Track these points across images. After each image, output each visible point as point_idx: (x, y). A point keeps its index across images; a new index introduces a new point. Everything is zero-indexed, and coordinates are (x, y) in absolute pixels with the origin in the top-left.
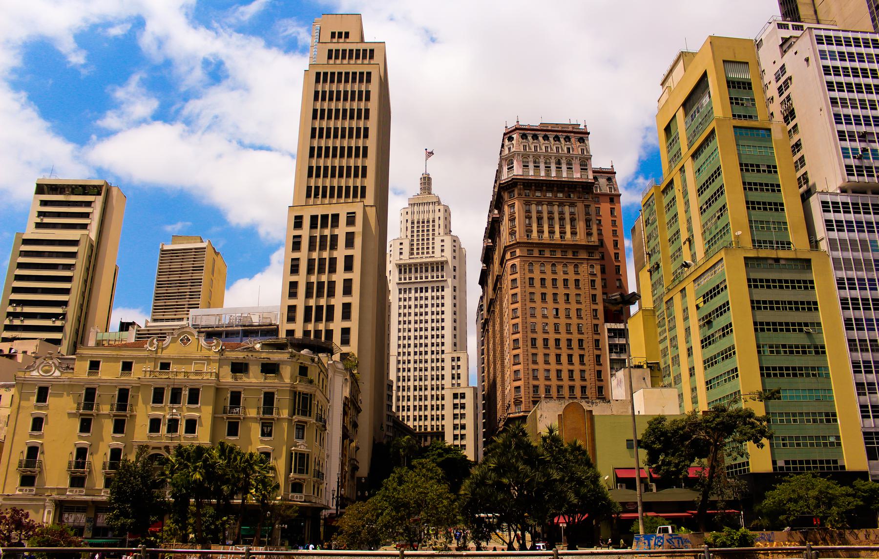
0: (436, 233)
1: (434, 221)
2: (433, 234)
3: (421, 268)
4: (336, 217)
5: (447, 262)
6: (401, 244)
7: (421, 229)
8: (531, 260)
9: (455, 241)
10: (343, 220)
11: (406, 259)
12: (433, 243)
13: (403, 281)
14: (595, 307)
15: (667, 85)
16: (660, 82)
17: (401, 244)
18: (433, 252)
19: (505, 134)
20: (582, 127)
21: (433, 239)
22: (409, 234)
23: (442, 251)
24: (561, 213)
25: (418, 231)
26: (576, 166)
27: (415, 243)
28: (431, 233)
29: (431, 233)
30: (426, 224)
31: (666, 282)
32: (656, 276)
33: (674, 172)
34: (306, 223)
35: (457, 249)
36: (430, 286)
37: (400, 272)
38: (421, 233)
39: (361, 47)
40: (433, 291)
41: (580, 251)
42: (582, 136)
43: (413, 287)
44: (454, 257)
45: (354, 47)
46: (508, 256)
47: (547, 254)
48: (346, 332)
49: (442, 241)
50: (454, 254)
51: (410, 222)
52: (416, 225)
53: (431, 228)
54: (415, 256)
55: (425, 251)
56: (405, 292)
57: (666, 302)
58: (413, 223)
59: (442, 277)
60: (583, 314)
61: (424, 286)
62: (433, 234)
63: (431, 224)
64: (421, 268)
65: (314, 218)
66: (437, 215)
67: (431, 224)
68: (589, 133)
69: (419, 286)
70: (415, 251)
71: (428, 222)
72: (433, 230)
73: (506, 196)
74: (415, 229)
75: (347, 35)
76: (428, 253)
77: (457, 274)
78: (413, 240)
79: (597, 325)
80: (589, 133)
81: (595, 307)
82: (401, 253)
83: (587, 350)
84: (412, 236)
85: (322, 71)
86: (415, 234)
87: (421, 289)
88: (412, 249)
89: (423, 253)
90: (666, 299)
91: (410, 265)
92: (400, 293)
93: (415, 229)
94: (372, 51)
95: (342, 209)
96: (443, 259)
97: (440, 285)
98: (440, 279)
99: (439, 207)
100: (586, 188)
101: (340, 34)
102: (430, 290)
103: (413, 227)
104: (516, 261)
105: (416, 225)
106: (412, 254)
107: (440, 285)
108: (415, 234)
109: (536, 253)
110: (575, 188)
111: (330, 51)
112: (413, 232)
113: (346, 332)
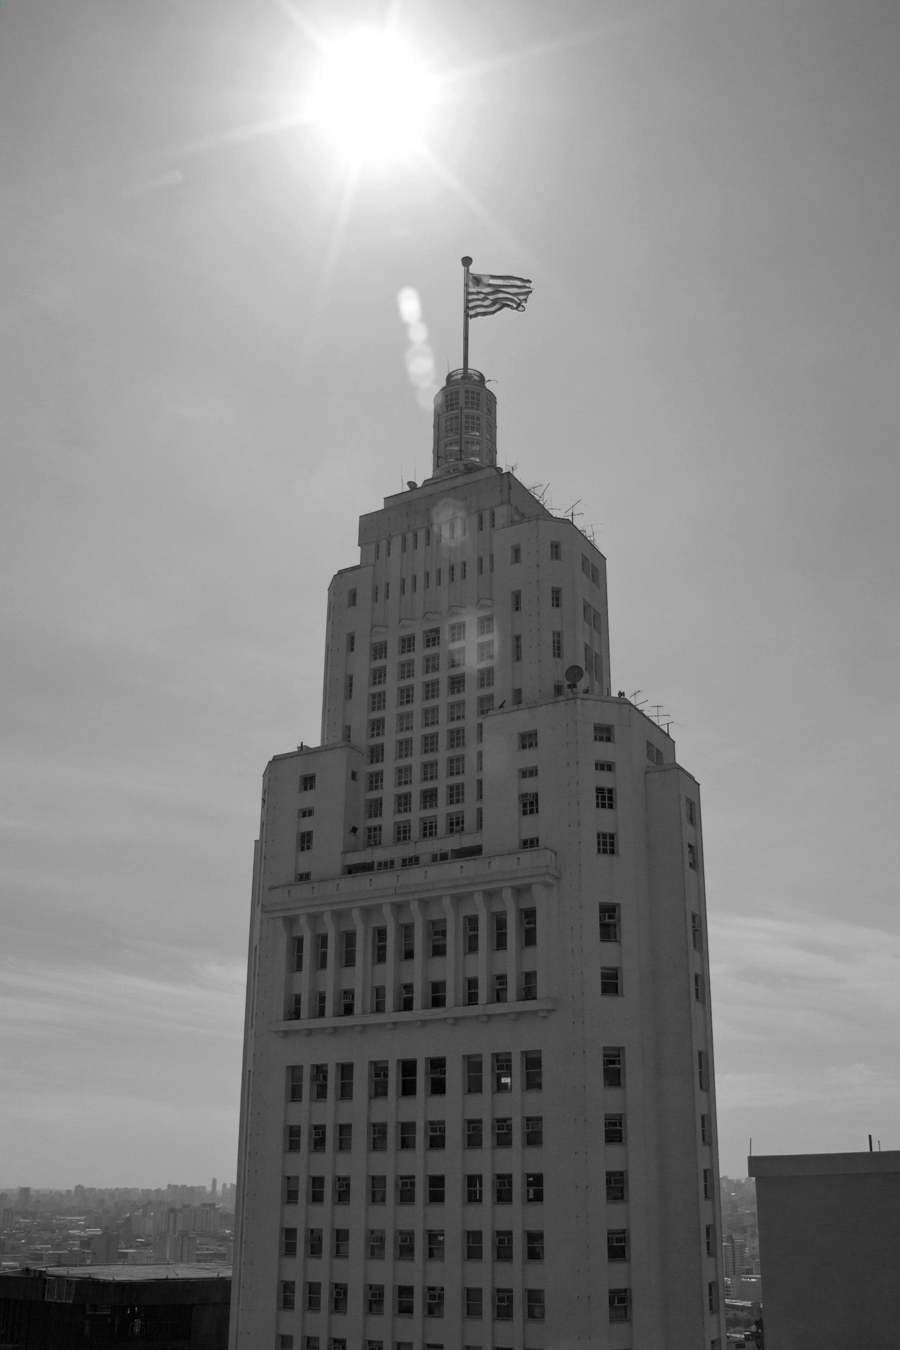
23: (529, 805)
25: (406, 695)
44: (607, 844)
49: (528, 740)
50: (605, 821)
52: (392, 661)
58: (379, 651)
69: (392, 1050)
70: (388, 820)
74: (392, 685)
77: (629, 955)
78: (376, 753)
82: (305, 841)
84: (377, 726)
88: (375, 808)
93: (392, 685)
97: (515, 1041)
103: (378, 676)
108: (391, 712)
112: (377, 702)
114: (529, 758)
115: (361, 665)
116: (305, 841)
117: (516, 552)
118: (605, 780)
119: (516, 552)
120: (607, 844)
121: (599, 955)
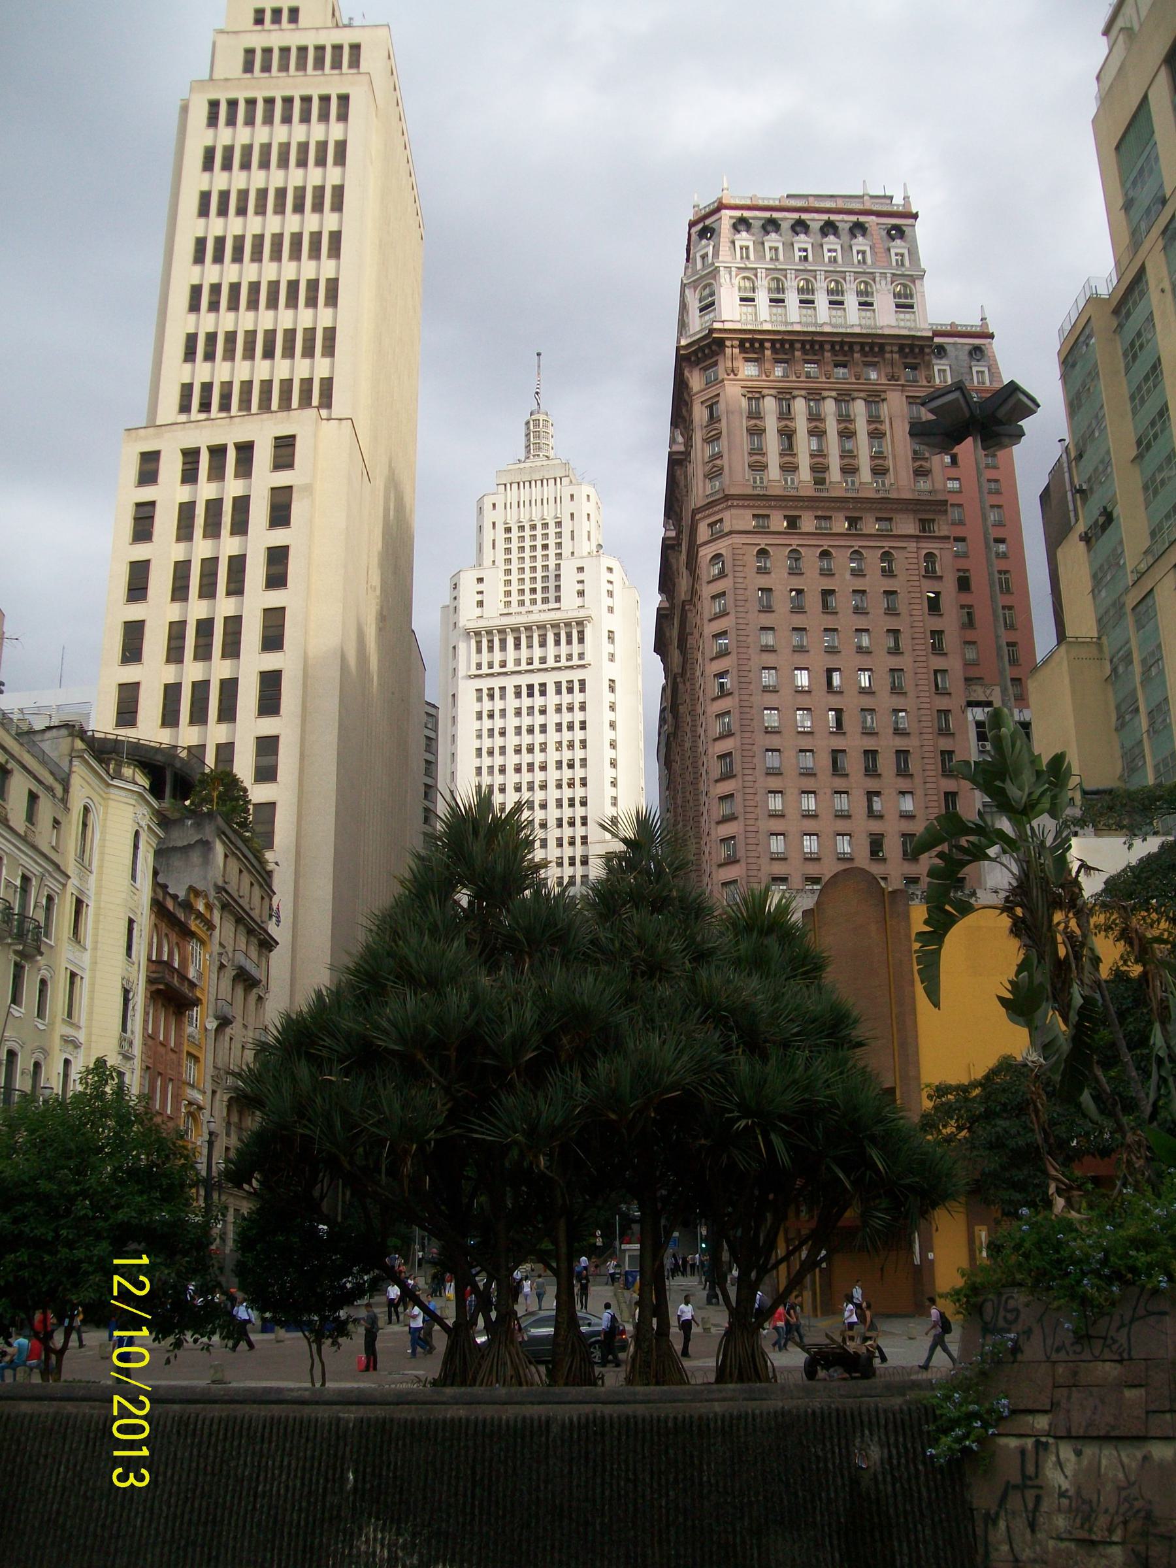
0: (566, 551)
1: (559, 524)
2: (559, 556)
3: (530, 638)
4: (245, 450)
5: (589, 618)
6: (480, 580)
7: (527, 544)
8: (763, 541)
9: (610, 570)
10: (263, 456)
11: (493, 615)
12: (558, 577)
13: (485, 670)
14: (938, 663)
15: (1120, 23)
16: (1102, 25)
17: (480, 580)
18: (558, 599)
19: (692, 225)
20: (898, 200)
21: (558, 566)
22: (501, 556)
23: (581, 593)
24: (845, 419)
26: (884, 301)
27: (515, 577)
28: (552, 551)
29: (552, 551)
30: (539, 532)
31: (1132, 559)
32: (1105, 544)
33: (1146, 246)
34: (171, 467)
35: (617, 588)
36: (550, 679)
37: (479, 651)
38: (527, 554)
39: (329, 38)
40: (559, 692)
41: (897, 517)
42: (899, 224)
43: (510, 683)
44: (611, 610)
45: (310, 40)
46: (703, 533)
47: (808, 523)
48: (267, 746)
51: (500, 528)
52: (515, 534)
53: (552, 541)
54: (515, 607)
55: (539, 596)
56: (491, 697)
57: (1133, 609)
58: (508, 530)
59: (581, 656)
60: (908, 682)
61: (536, 679)
62: (559, 556)
63: (552, 530)
64: (530, 638)
65: (191, 456)
66: (567, 507)
67: (552, 530)
68: (915, 216)
69: (523, 681)
70: (515, 598)
71: (545, 526)
72: (559, 545)
73: (696, 381)
74: (515, 545)
75: (294, 13)
76: (545, 601)
79: (947, 712)
80: (915, 216)
81: (938, 663)
82: (480, 604)
83: (918, 780)
84: (508, 561)
85: (223, 97)
86: (515, 555)
87: (530, 687)
88: (508, 593)
89: (534, 602)
90: (1131, 600)
91: (502, 631)
92: (480, 699)
93: (515, 545)
94: (356, 48)
95: (262, 431)
96: (582, 613)
97: (576, 675)
98: (575, 661)
99: (572, 490)
100: (916, 351)
101: (277, 12)
102: (551, 689)
103: (508, 540)
104: (721, 546)
105: (515, 534)
106: (508, 604)
107: (576, 675)
108: (515, 555)
109: (778, 522)
110: (882, 347)
111: (250, 52)
113: (267, 746)
114: (581, 577)
115: (501, 535)
116: (480, 604)
117: (572, 496)
118: (610, 587)
119: (572, 496)
120: (611, 610)
121: (607, 648)
